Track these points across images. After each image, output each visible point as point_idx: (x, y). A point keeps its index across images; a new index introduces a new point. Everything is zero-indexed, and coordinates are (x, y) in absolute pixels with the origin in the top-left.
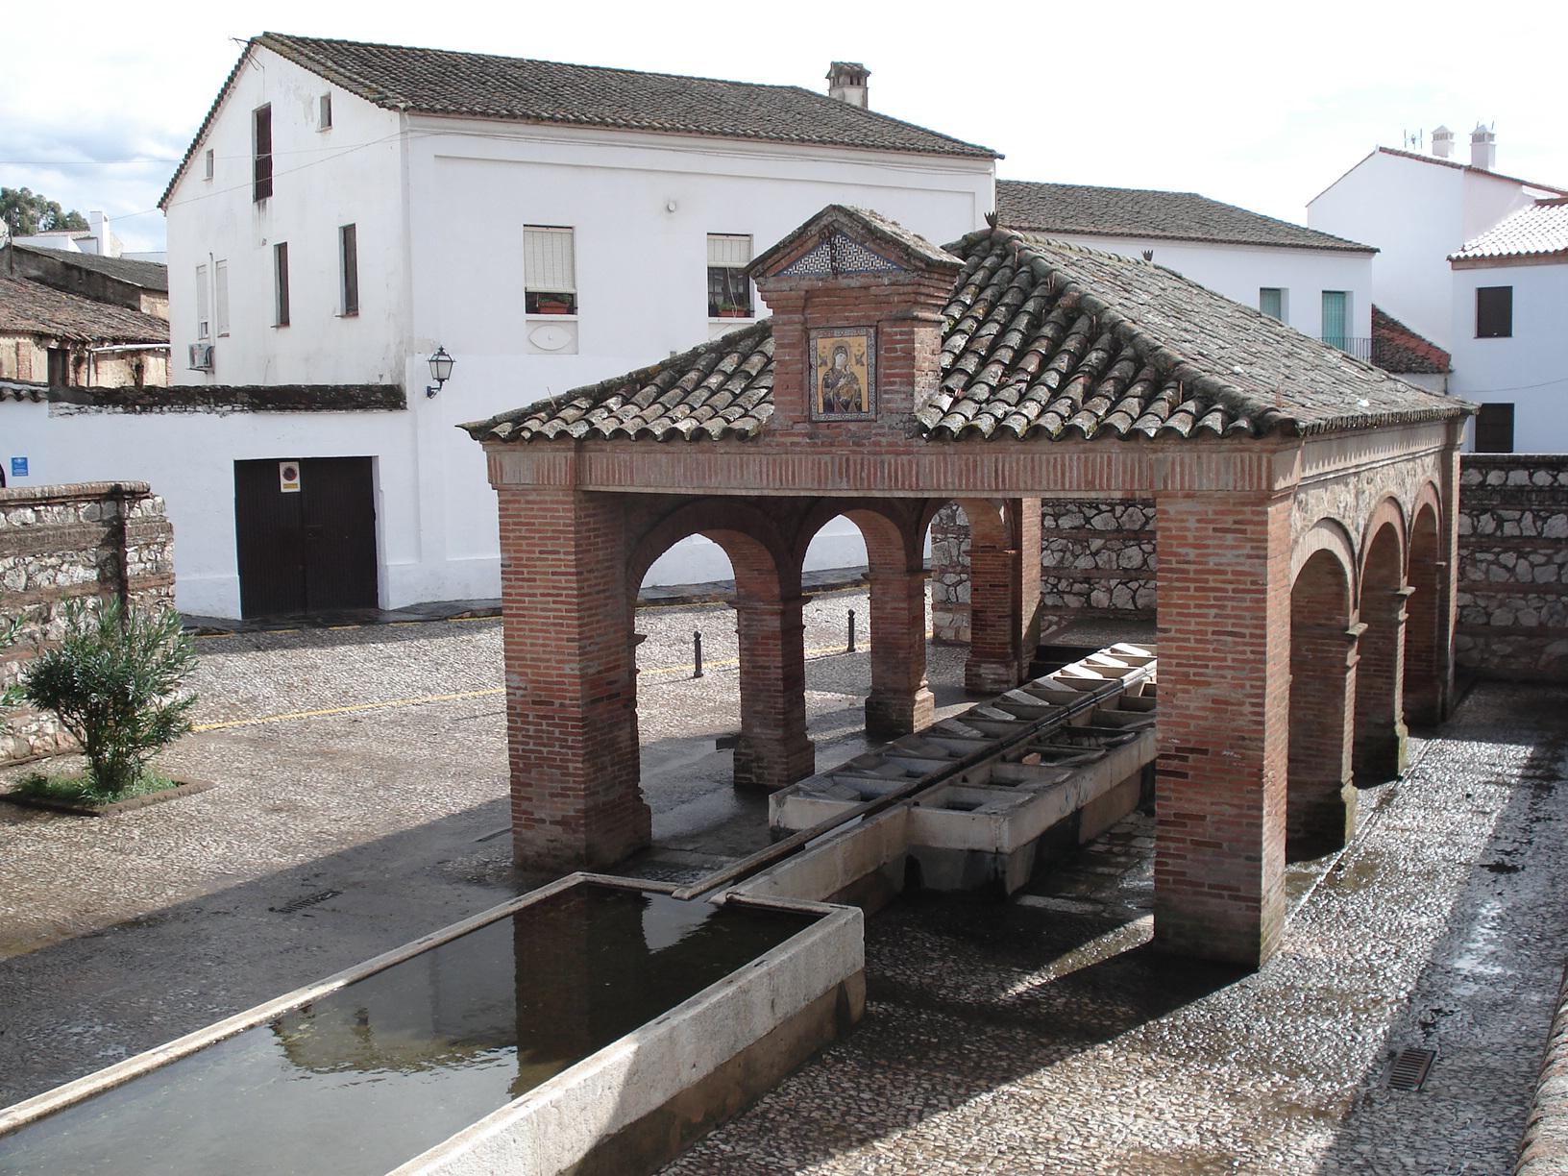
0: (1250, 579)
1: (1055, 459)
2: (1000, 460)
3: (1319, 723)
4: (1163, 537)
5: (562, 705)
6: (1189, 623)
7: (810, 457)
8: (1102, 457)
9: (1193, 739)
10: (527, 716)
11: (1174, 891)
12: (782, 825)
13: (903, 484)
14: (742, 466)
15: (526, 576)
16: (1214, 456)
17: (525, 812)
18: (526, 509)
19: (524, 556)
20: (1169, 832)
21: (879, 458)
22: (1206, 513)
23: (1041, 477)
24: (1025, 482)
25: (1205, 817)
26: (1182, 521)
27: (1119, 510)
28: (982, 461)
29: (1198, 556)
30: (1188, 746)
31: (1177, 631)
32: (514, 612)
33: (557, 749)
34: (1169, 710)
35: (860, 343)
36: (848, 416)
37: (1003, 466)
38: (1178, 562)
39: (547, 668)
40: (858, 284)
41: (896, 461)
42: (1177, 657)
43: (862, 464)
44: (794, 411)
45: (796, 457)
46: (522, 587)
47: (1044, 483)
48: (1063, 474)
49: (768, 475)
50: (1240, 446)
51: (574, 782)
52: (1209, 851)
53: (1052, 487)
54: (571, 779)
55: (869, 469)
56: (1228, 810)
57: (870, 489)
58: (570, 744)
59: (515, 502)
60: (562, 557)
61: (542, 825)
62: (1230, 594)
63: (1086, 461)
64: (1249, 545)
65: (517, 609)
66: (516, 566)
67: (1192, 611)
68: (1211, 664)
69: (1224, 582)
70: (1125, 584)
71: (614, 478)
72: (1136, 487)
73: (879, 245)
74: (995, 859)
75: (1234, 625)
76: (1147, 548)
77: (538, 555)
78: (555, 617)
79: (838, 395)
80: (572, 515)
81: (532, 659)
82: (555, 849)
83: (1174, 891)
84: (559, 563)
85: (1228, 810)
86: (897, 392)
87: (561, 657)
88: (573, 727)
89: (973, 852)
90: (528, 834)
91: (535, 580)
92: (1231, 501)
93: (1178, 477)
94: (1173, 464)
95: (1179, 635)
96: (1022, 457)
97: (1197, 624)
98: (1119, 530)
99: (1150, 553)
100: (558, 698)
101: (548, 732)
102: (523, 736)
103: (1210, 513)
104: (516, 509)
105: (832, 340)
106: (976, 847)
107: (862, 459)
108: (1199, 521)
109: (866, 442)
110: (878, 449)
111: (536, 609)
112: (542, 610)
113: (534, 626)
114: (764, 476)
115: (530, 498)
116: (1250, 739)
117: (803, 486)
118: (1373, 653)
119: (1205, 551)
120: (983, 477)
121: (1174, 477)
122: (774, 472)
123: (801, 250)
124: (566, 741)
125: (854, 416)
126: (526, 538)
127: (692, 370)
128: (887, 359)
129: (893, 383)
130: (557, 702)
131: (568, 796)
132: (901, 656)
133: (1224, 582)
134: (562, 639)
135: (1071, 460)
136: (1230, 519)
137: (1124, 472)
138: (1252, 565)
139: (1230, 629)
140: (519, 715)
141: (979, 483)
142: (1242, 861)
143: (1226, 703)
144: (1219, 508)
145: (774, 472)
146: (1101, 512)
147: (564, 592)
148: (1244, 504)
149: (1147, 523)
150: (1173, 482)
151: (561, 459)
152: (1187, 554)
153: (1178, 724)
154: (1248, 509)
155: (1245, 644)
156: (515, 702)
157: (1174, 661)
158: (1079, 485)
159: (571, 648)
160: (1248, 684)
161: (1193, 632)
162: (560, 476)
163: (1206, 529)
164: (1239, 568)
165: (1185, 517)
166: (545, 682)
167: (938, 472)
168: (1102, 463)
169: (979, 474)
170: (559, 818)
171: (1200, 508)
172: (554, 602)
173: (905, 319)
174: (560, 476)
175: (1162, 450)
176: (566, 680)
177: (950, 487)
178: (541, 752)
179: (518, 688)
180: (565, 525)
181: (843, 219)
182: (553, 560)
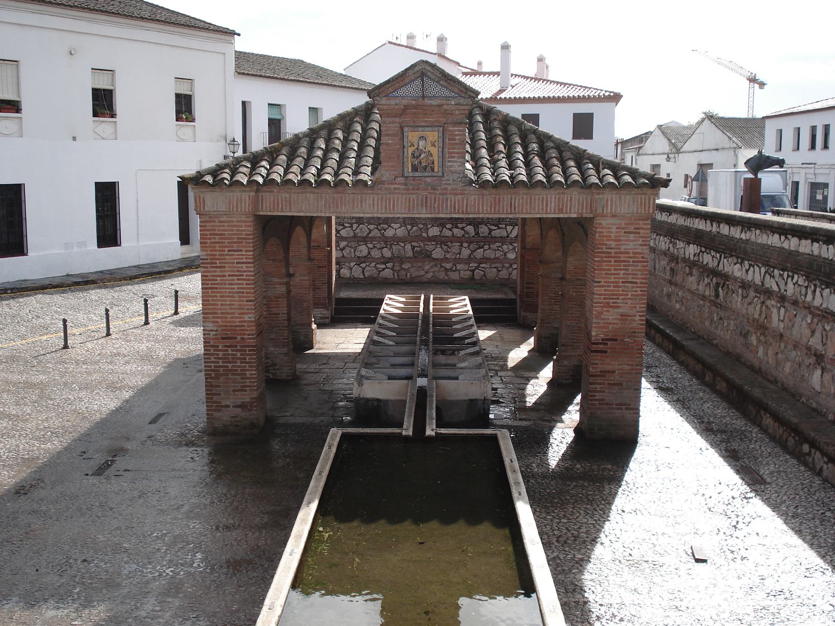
0: (641, 255)
1: (543, 198)
2: (513, 198)
3: (578, 327)
4: (599, 236)
5: (242, 339)
6: (611, 278)
7: (404, 197)
8: (567, 197)
9: (611, 334)
10: (218, 346)
11: (599, 409)
12: (361, 396)
13: (458, 210)
14: (361, 201)
15: (218, 265)
16: (628, 196)
17: (215, 402)
18: (220, 226)
19: (217, 253)
20: (597, 380)
21: (445, 197)
22: (621, 224)
23: (535, 207)
24: (527, 209)
25: (614, 372)
26: (609, 228)
27: (355, 226)
28: (503, 199)
29: (616, 245)
30: (608, 338)
31: (605, 282)
32: (209, 286)
33: (238, 364)
34: (600, 321)
35: (433, 135)
36: (426, 174)
37: (515, 201)
38: (606, 248)
39: (233, 318)
40: (437, 103)
41: (454, 198)
42: (605, 295)
43: (435, 200)
44: (395, 170)
45: (396, 196)
46: (215, 272)
47: (537, 209)
48: (547, 205)
49: (378, 206)
50: (641, 192)
51: (250, 382)
52: (616, 388)
53: (540, 211)
54: (248, 381)
55: (439, 202)
56: (626, 367)
57: (439, 213)
58: (247, 360)
59: (211, 222)
60: (244, 253)
61: (228, 409)
62: (631, 263)
63: (559, 199)
64: (641, 239)
65: (212, 284)
66: (211, 259)
67: (612, 272)
68: (620, 297)
69: (628, 257)
70: (359, 265)
71: (278, 207)
72: (584, 211)
73: (449, 83)
74: (484, 403)
75: (632, 278)
76: (370, 246)
77: (227, 252)
78: (238, 288)
79: (420, 163)
80: (251, 229)
81: (222, 313)
82: (236, 421)
83: (599, 409)
84: (241, 257)
85: (626, 367)
86: (456, 162)
87: (242, 311)
88: (249, 351)
89: (471, 400)
90: (217, 414)
91: (225, 267)
92: (633, 218)
93: (609, 207)
94: (607, 201)
95: (605, 284)
96: (525, 196)
97: (615, 278)
98: (355, 236)
99: (372, 249)
100: (241, 334)
101: (232, 355)
102: (215, 358)
103: (623, 224)
104: (212, 226)
105: (418, 133)
106: (473, 398)
107: (435, 198)
108: (617, 228)
109: (439, 188)
110: (445, 192)
111: (225, 284)
112: (230, 284)
113: (224, 294)
114: (376, 207)
115: (222, 219)
116: (638, 333)
117: (400, 211)
118: (554, 294)
119: (620, 243)
120: (503, 207)
121: (607, 206)
122: (382, 204)
123: (402, 84)
124: (245, 359)
125: (430, 174)
126: (219, 243)
127: (300, 147)
128: (450, 144)
129: (453, 157)
130: (239, 337)
131: (246, 391)
132: (305, 305)
133: (628, 257)
134: (243, 301)
135: (551, 198)
136: (632, 227)
137: (579, 204)
138: (642, 249)
139: (630, 280)
140: (212, 346)
141: (501, 210)
142: (632, 391)
143: (628, 316)
144: (627, 222)
145: (382, 204)
146: (345, 227)
147: (245, 274)
148: (640, 220)
149: (370, 232)
150: (607, 209)
151: (247, 197)
152: (611, 244)
153: (604, 327)
154: (641, 222)
155: (637, 287)
156: (210, 339)
157: (603, 297)
158: (555, 211)
159: (250, 305)
160: (638, 306)
161: (612, 282)
162: (245, 206)
163: (621, 232)
164: (636, 251)
165: (610, 226)
166: (231, 326)
167: (479, 204)
168: (567, 201)
169: (501, 205)
170: (240, 404)
171: (618, 222)
172: (238, 280)
173: (461, 123)
174: (245, 206)
175: (603, 193)
176: (245, 324)
177: (485, 212)
178: (227, 367)
179: (212, 331)
180: (247, 235)
181: (428, 68)
182: (237, 255)
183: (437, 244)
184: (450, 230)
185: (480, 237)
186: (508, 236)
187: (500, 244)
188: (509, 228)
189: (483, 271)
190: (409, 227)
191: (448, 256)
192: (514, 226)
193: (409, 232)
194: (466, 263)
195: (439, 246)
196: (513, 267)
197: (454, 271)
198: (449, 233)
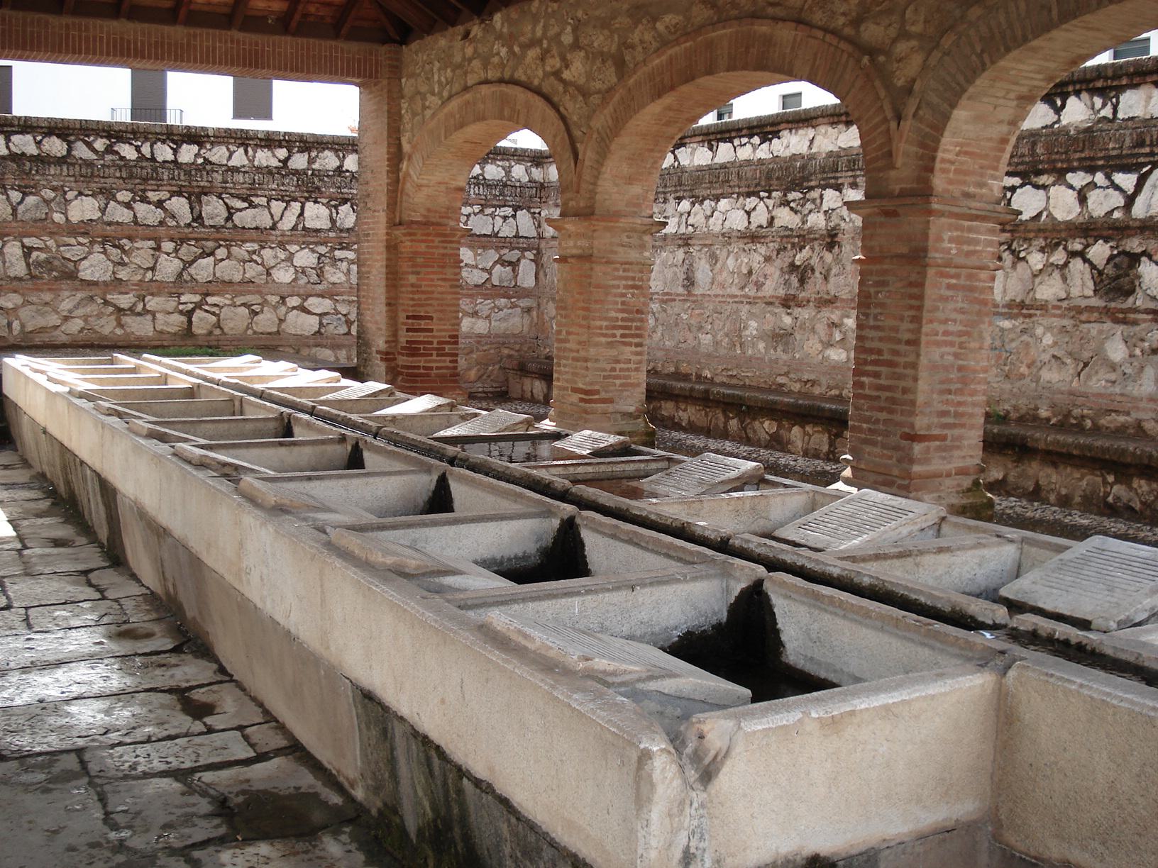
3: (960, 369)
118: (622, 311)
183: (92, 243)
184: (128, 206)
185: (202, 225)
186: (274, 227)
187: (256, 247)
188: (277, 206)
189: (214, 314)
190: (15, 196)
191: (123, 274)
192: (288, 203)
193: (14, 210)
194: (171, 294)
195: (97, 248)
196: (288, 304)
197: (139, 314)
198: (123, 215)
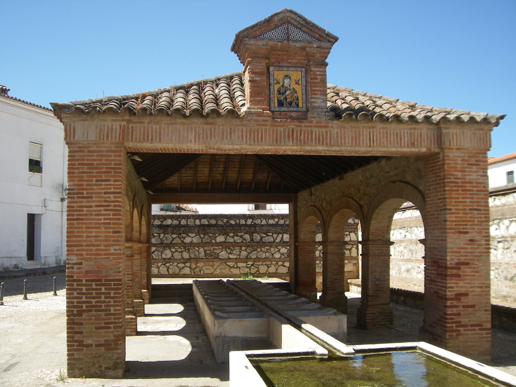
4: (448, 167)
15: (85, 195)
18: (89, 156)
19: (85, 183)
27: (162, 235)
28: (363, 132)
32: (75, 217)
33: (103, 299)
36: (291, 109)
38: (455, 178)
42: (456, 221)
53: (396, 145)
54: (112, 317)
60: (112, 183)
62: (475, 192)
65: (78, 215)
67: (461, 200)
68: (469, 223)
69: (473, 187)
70: (164, 264)
76: (173, 250)
77: (94, 182)
78: (105, 219)
81: (87, 246)
84: (110, 187)
86: (319, 98)
87: (108, 243)
95: (456, 211)
98: (162, 243)
99: (174, 252)
103: (466, 157)
104: (81, 156)
112: (96, 215)
113: (89, 225)
114: (244, 138)
120: (363, 140)
122: (250, 136)
125: (295, 109)
129: (316, 94)
131: (110, 328)
132: (136, 280)
133: (473, 187)
134: (109, 232)
136: (474, 159)
137: (427, 139)
139: (476, 208)
142: (483, 312)
145: (250, 136)
146: (154, 236)
147: (112, 204)
148: (479, 153)
149: (173, 240)
152: (458, 175)
155: (482, 214)
157: (454, 223)
158: (408, 145)
161: (461, 210)
165: (456, 158)
168: (418, 135)
169: (361, 139)
172: (105, 210)
182: (105, 185)
183: (223, 248)
184: (232, 237)
185: (253, 242)
186: (274, 242)
187: (269, 247)
188: (275, 236)
189: (257, 267)
190: (202, 236)
191: (231, 256)
192: (278, 234)
193: (202, 240)
194: (244, 262)
195: (224, 249)
196: (279, 264)
197: (236, 268)
198: (232, 240)
